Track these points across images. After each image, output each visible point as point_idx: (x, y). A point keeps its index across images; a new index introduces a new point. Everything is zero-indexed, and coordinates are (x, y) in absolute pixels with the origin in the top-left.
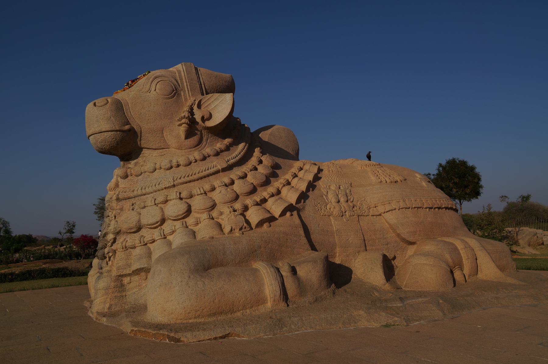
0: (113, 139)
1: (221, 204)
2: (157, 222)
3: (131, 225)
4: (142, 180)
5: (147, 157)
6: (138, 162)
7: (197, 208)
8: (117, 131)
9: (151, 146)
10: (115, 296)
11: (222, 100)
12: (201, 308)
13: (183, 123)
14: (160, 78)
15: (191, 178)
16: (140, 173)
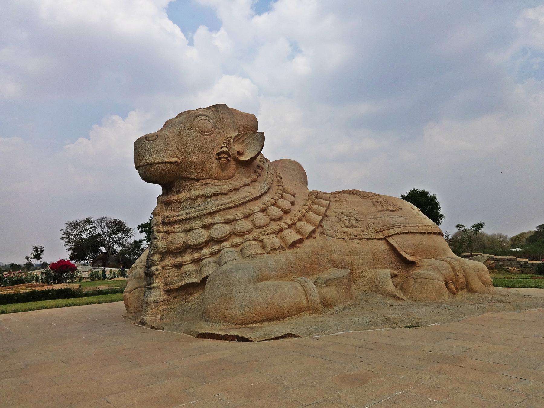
0: (162, 170)
1: (258, 228)
2: (203, 243)
3: (178, 246)
4: (185, 207)
5: (189, 186)
6: (179, 190)
7: (238, 231)
8: (166, 163)
9: (193, 176)
10: (165, 308)
11: (254, 138)
12: (256, 314)
13: (224, 157)
14: (201, 117)
15: (230, 205)
16: (183, 200)
